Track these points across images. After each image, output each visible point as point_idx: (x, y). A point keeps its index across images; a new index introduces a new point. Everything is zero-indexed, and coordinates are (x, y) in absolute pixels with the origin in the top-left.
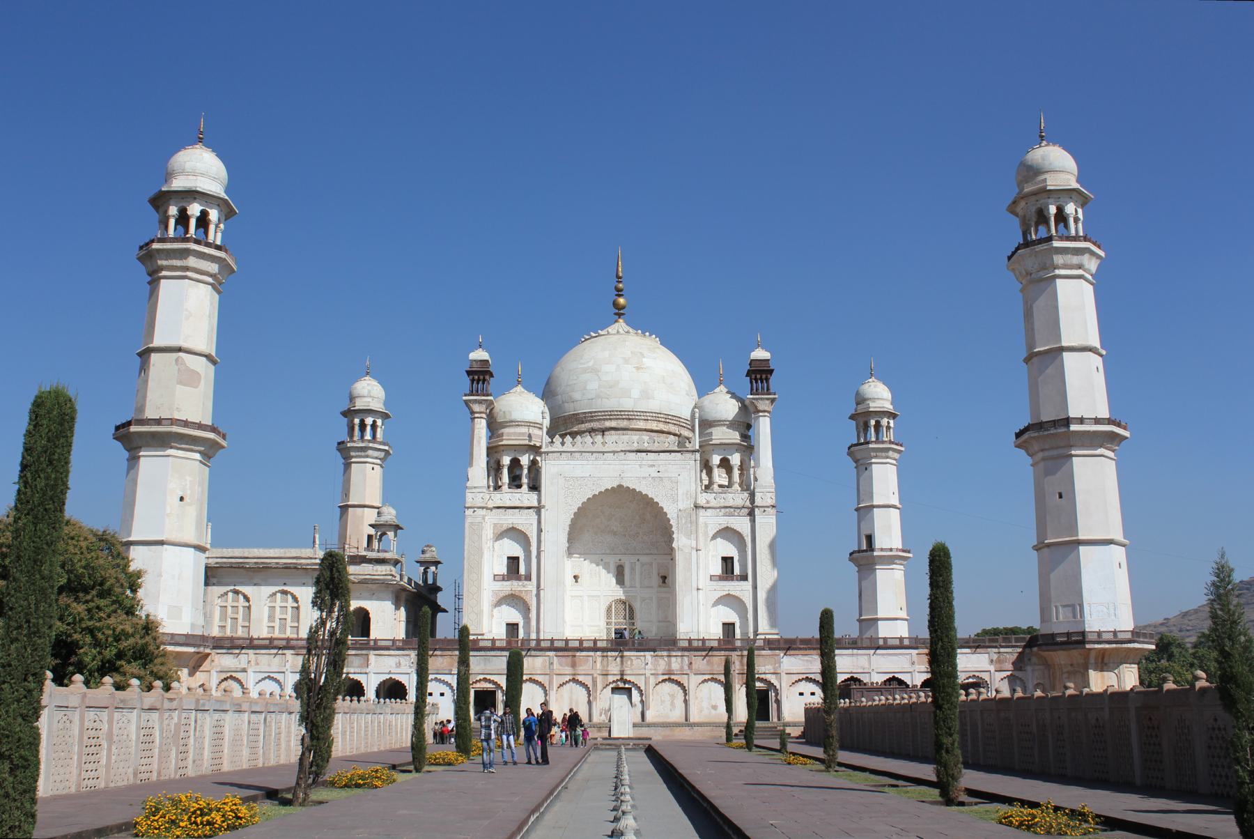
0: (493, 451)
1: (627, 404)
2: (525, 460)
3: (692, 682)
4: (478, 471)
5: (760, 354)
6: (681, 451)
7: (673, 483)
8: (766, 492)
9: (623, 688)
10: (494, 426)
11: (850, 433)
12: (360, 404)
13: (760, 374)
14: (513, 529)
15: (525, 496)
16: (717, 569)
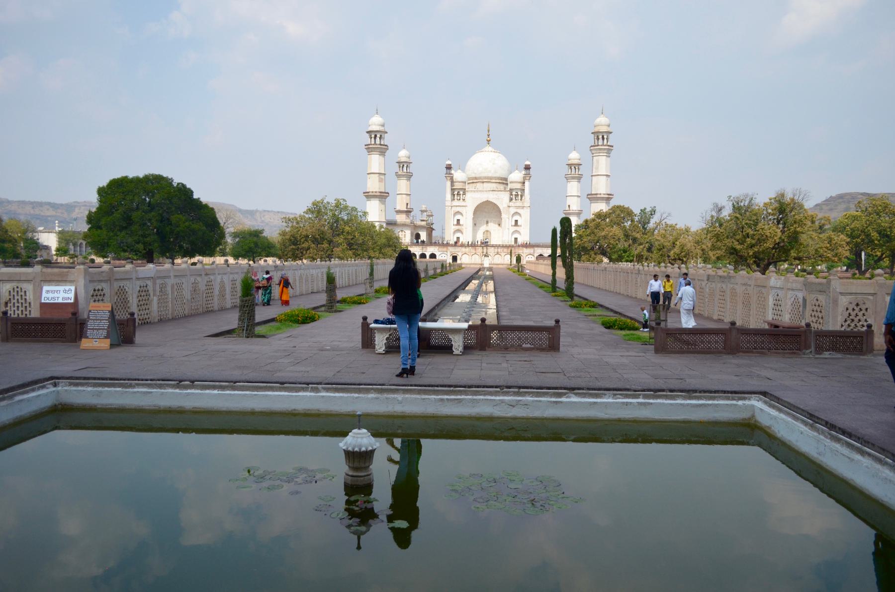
0: (453, 190)
1: (490, 175)
2: (461, 193)
3: (503, 254)
4: (449, 196)
5: (528, 163)
6: (505, 190)
7: (501, 199)
8: (527, 204)
9: (486, 256)
10: (452, 182)
11: (566, 170)
12: (403, 160)
13: (527, 168)
14: (458, 213)
15: (461, 203)
16: (513, 223)
